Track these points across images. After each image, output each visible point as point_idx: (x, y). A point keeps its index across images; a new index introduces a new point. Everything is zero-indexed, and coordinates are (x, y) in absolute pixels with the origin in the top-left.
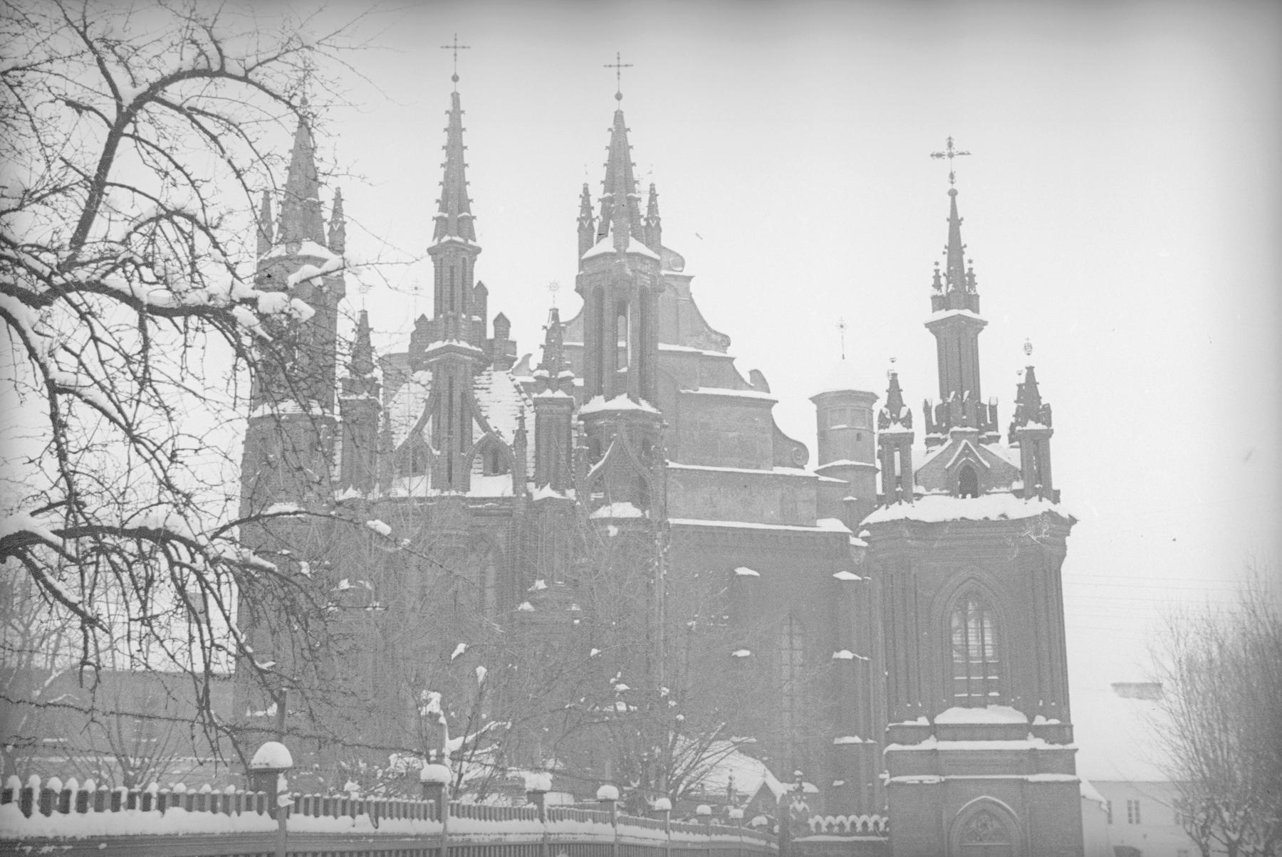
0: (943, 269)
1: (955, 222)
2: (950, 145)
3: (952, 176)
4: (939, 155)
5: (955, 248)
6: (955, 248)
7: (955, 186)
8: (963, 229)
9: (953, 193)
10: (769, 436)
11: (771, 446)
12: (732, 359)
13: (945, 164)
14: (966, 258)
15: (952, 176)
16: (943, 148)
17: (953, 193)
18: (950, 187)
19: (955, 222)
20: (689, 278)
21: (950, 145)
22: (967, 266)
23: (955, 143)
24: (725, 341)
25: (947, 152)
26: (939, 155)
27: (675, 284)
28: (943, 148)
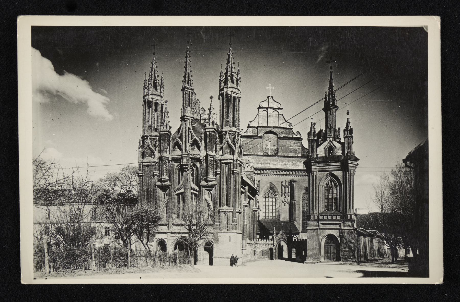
10: (301, 148)
11: (301, 150)
27: (278, 111)
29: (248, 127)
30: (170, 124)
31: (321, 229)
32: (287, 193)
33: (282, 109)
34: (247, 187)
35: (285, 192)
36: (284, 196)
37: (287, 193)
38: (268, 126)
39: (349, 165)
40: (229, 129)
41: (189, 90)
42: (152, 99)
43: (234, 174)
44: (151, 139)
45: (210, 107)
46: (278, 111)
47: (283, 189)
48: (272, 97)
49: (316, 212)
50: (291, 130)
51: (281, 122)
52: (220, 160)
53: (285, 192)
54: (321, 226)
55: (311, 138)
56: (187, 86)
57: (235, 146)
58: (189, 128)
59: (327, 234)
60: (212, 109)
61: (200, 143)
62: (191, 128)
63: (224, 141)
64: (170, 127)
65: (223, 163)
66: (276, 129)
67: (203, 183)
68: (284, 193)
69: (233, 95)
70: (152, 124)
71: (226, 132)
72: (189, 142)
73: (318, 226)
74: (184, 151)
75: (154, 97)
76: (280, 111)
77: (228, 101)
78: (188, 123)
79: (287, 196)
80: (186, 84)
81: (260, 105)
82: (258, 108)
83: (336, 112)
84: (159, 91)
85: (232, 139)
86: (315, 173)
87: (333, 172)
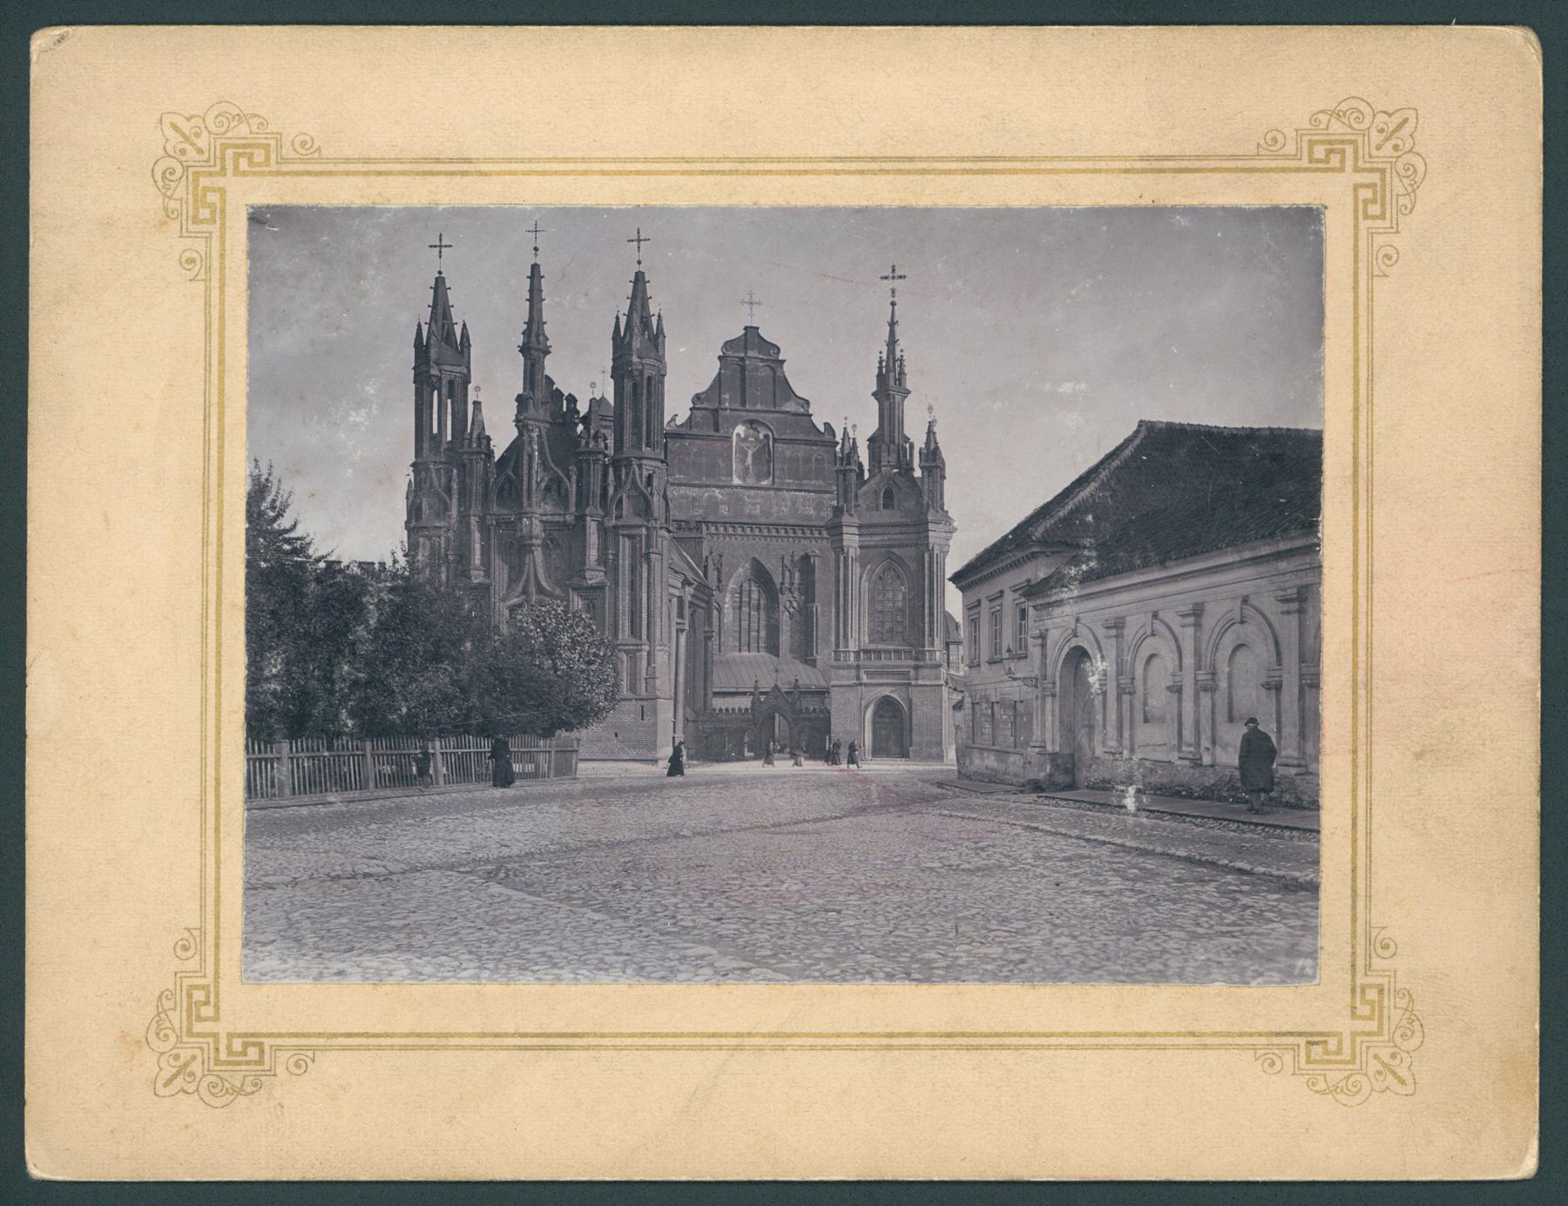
0: (884, 356)
1: (892, 324)
2: (893, 271)
3: (893, 291)
4: (886, 278)
5: (892, 342)
6: (892, 342)
7: (896, 299)
8: (897, 329)
9: (893, 304)
12: (811, 415)
13: (890, 284)
14: (898, 349)
15: (893, 291)
16: (889, 273)
17: (893, 304)
18: (892, 299)
19: (892, 324)
20: (784, 361)
21: (893, 271)
22: (898, 355)
24: (807, 402)
25: (891, 275)
26: (886, 278)
28: (889, 273)
31: (866, 685)
32: (796, 585)
33: (784, 361)
35: (792, 584)
37: (796, 585)
47: (787, 573)
48: (757, 328)
49: (853, 647)
50: (807, 418)
52: (615, 527)
54: (865, 679)
65: (623, 535)
68: (787, 585)
73: (858, 678)
82: (720, 358)
83: (903, 401)
86: (851, 550)
87: (895, 550)
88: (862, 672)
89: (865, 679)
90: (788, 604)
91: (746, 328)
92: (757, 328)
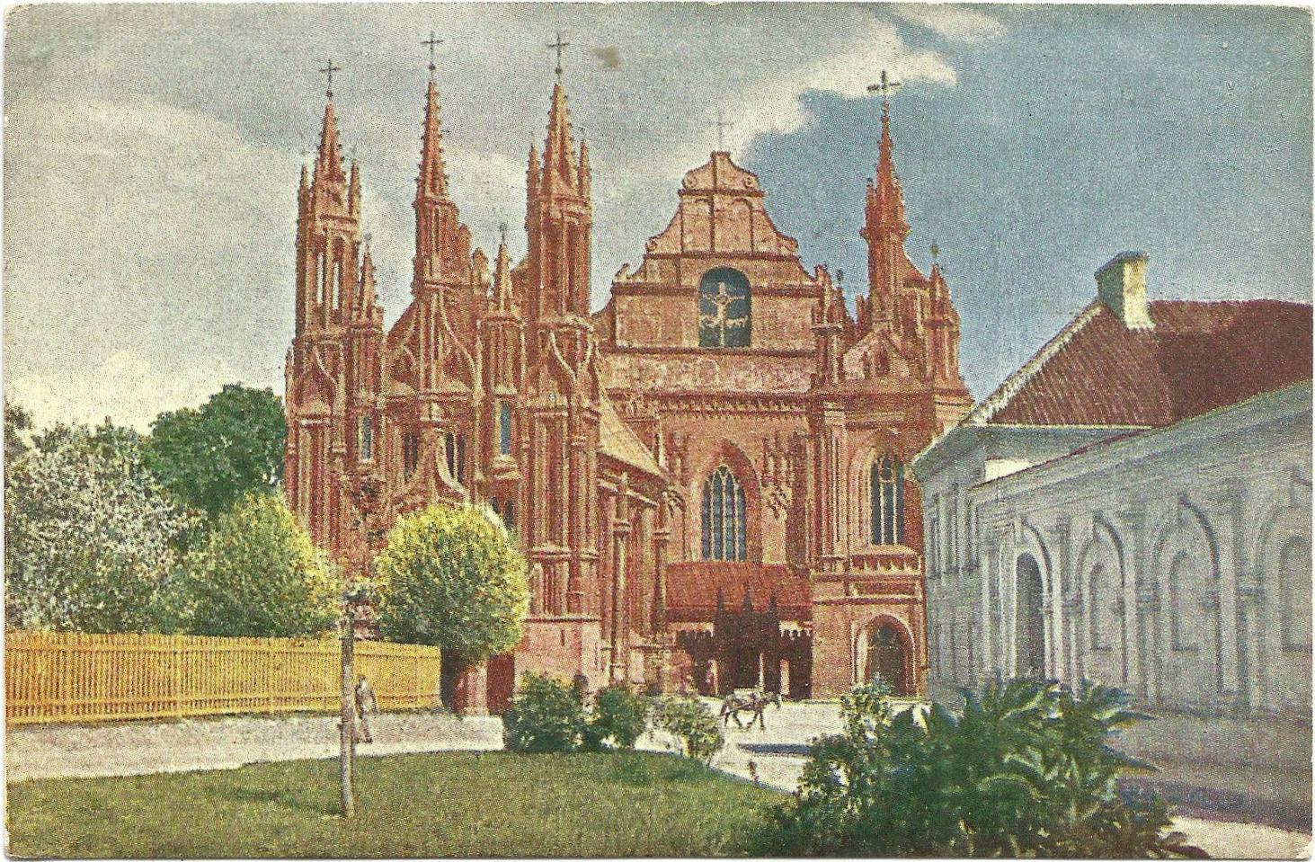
23: (872, 83)
29: (645, 258)
30: (378, 303)
34: (624, 477)
36: (771, 486)
38: (717, 250)
39: (938, 407)
40: (557, 319)
41: (438, 207)
42: (325, 230)
43: (572, 450)
44: (321, 348)
45: (500, 255)
46: (747, 198)
47: (771, 462)
51: (758, 235)
52: (530, 410)
53: (777, 472)
55: (820, 326)
56: (429, 194)
57: (575, 370)
58: (438, 315)
59: (866, 620)
60: (505, 260)
61: (472, 363)
62: (443, 312)
63: (544, 355)
64: (380, 311)
66: (744, 263)
67: (479, 476)
69: (567, 219)
70: (324, 304)
71: (546, 327)
72: (436, 358)
74: (422, 384)
75: (330, 224)
76: (755, 202)
77: (554, 241)
78: (434, 305)
79: (783, 486)
80: (428, 188)
81: (687, 184)
84: (346, 204)
85: (565, 349)
86: (836, 433)
88: (852, 586)
89: (855, 595)
90: (772, 499)
91: (713, 155)
92: (727, 155)
